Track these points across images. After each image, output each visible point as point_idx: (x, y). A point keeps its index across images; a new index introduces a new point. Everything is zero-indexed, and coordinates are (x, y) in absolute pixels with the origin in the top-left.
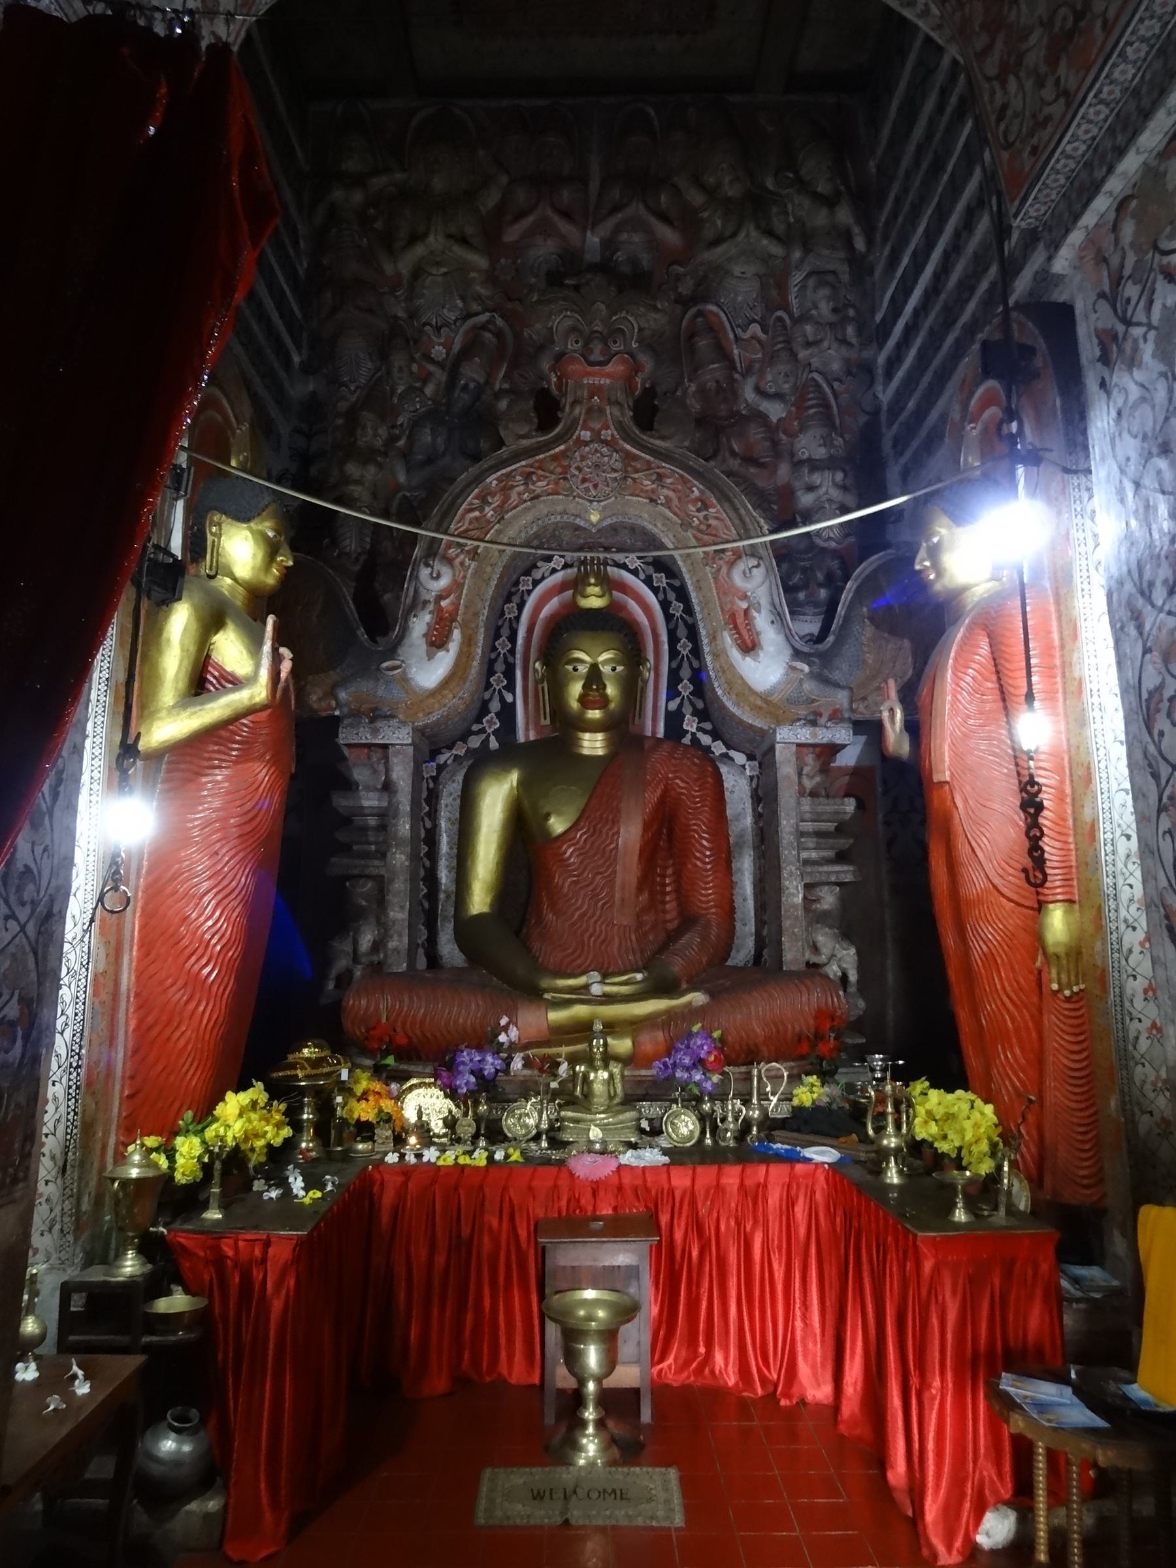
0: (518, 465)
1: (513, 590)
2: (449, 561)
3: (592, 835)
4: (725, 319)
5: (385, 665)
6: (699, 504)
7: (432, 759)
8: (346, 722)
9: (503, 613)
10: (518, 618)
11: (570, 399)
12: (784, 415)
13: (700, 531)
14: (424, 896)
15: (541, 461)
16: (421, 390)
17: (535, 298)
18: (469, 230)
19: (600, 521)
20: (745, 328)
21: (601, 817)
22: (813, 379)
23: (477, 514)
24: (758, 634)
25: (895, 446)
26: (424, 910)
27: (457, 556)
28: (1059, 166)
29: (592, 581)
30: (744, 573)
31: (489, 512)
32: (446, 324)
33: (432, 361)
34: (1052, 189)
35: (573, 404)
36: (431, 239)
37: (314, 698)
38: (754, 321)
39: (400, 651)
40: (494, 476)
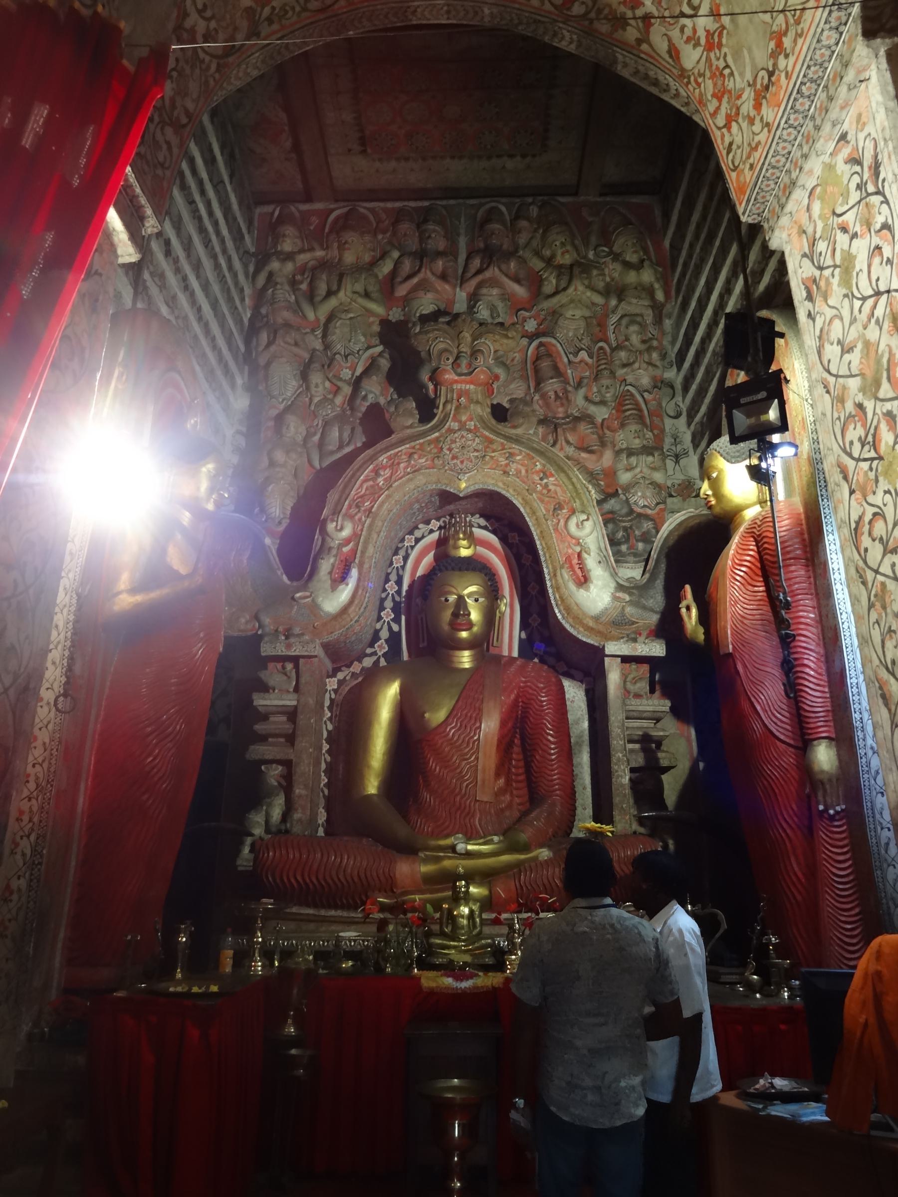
0: (403, 447)
1: (400, 545)
2: (352, 517)
3: (459, 729)
4: (560, 348)
5: (298, 595)
6: (542, 475)
7: (334, 675)
8: (266, 639)
9: (391, 563)
10: (403, 567)
11: (443, 400)
12: (606, 416)
13: (543, 495)
14: (324, 785)
15: (421, 445)
16: (332, 401)
17: (418, 330)
18: (371, 288)
19: (466, 487)
20: (576, 354)
21: (466, 715)
22: (628, 391)
23: (371, 483)
24: (589, 571)
25: (693, 441)
26: (324, 795)
27: (356, 514)
28: (768, 175)
29: (461, 536)
30: (577, 525)
31: (381, 481)
32: (352, 353)
33: (341, 379)
34: (766, 192)
35: (444, 404)
36: (341, 294)
37: (243, 620)
38: (582, 349)
39: (310, 585)
40: (386, 455)
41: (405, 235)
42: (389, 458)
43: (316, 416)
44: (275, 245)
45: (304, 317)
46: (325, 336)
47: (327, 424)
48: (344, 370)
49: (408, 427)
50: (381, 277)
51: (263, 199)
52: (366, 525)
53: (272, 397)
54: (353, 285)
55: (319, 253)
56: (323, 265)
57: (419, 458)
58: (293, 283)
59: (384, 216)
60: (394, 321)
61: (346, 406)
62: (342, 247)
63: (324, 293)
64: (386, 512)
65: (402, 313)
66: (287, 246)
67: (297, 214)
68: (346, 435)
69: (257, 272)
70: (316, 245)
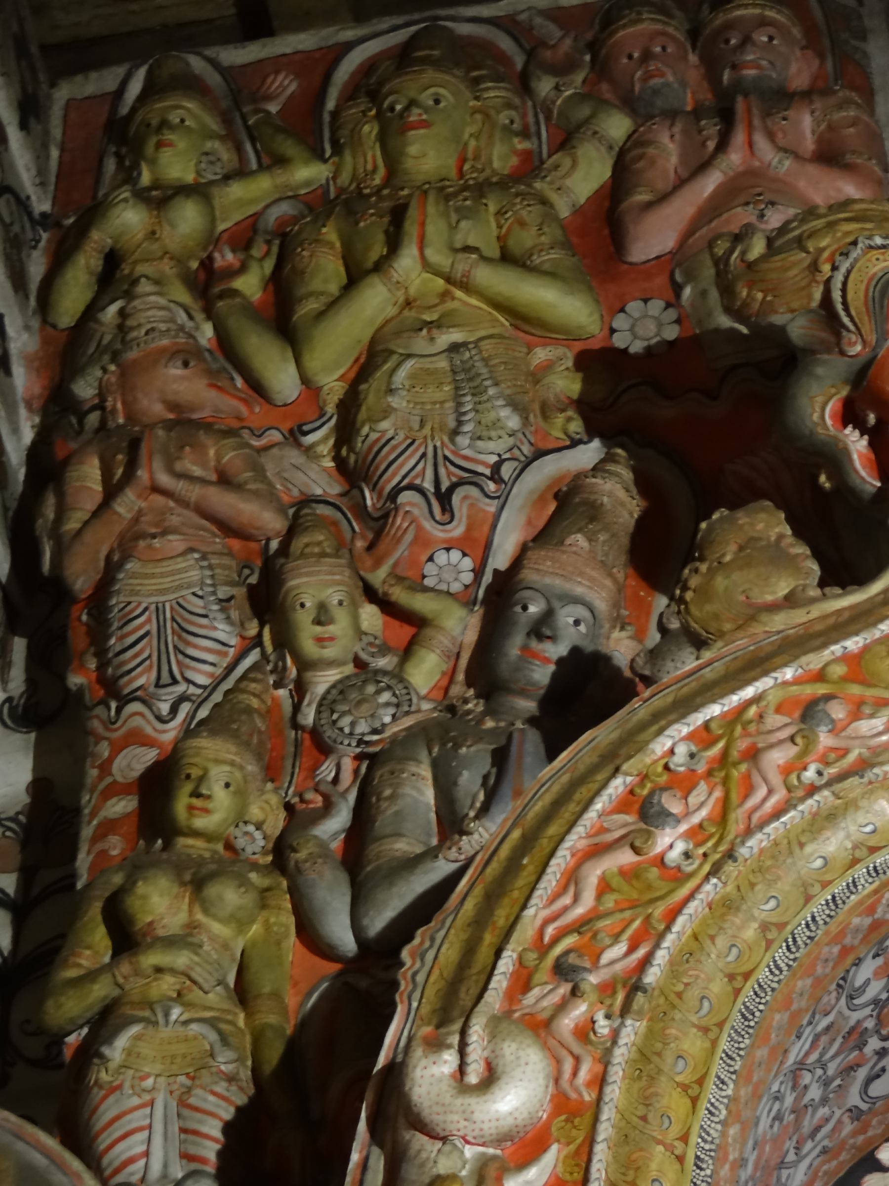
0: (765, 683)
2: (540, 1027)
15: (853, 660)
16: (398, 675)
18: (524, 240)
23: (625, 857)
27: (562, 1007)
31: (670, 843)
32: (472, 479)
33: (426, 590)
36: (407, 262)
40: (684, 729)
41: (647, 56)
42: (704, 736)
43: (324, 749)
44: (128, 175)
45: (258, 388)
46: (345, 433)
47: (376, 763)
48: (441, 558)
49: (773, 608)
50: (564, 212)
51: (79, 54)
52: (620, 1054)
53: (124, 700)
54: (453, 228)
55: (308, 173)
56: (319, 205)
57: (856, 715)
58: (207, 284)
59: (553, 31)
60: (637, 347)
61: (457, 690)
62: (393, 131)
63: (334, 288)
64: (718, 987)
65: (672, 314)
66: (176, 164)
67: (214, 79)
68: (470, 782)
69: (59, 261)
70: (288, 147)
